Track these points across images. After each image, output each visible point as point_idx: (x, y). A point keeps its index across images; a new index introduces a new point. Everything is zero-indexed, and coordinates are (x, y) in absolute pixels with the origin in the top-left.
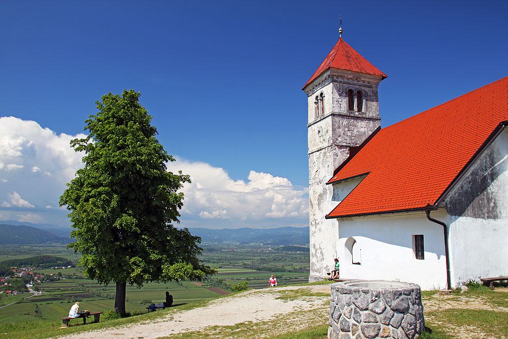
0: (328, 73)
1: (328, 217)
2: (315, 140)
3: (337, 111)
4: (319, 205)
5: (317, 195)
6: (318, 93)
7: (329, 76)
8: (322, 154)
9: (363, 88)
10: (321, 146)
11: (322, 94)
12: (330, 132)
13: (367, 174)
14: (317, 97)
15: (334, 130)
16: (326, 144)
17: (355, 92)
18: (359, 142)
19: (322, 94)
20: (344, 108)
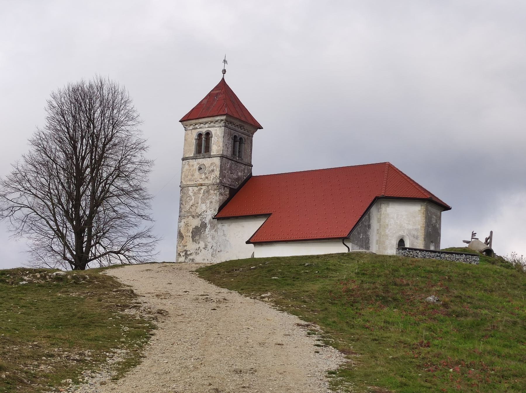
0: (224, 118)
1: (248, 242)
2: (193, 175)
3: (225, 154)
4: (193, 237)
5: (191, 229)
6: (204, 131)
7: (222, 120)
8: (202, 191)
9: (243, 135)
10: (201, 181)
11: (208, 134)
12: (217, 173)
13: (270, 214)
14: (200, 135)
15: (221, 171)
16: (206, 182)
17: (238, 138)
18: (237, 185)
19: (208, 134)
20: (229, 153)
